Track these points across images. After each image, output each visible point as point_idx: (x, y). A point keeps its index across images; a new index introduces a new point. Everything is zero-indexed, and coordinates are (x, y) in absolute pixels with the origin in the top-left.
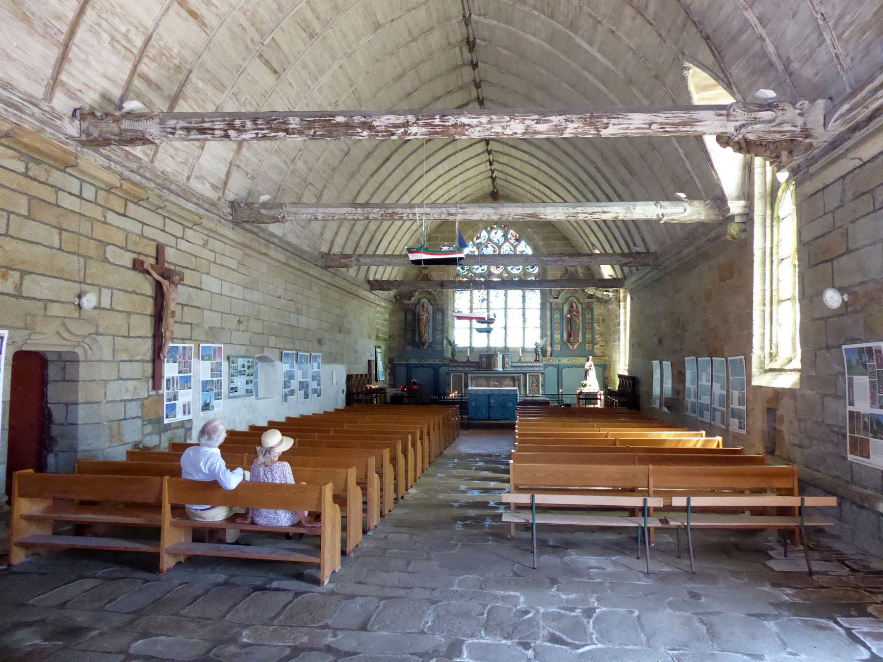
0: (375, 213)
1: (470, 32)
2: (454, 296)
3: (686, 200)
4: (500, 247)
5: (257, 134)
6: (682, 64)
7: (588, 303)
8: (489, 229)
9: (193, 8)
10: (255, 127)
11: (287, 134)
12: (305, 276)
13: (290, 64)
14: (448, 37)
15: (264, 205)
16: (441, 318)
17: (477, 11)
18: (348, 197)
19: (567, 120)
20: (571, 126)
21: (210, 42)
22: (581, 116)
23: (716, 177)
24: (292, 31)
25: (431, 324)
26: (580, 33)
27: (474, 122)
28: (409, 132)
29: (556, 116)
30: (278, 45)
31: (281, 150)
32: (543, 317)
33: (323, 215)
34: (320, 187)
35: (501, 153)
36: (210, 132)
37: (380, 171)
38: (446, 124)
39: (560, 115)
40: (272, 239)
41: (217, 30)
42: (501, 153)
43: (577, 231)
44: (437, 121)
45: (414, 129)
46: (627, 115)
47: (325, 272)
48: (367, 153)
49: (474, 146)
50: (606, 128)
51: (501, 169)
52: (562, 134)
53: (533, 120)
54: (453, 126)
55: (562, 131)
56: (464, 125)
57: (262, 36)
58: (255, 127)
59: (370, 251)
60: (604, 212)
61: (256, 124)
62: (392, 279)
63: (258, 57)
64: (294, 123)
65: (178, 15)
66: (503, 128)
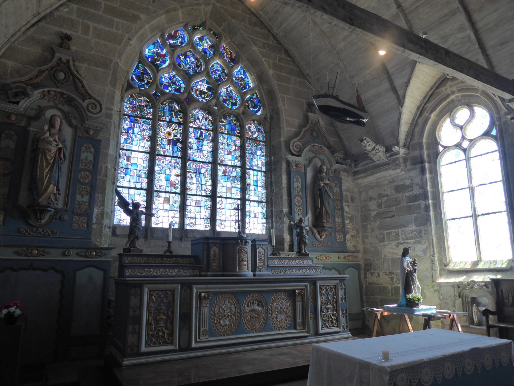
2: (120, 123)
4: (207, 63)
7: (335, 171)
8: (190, 28)
16: (91, 157)
25: (65, 167)
32: (269, 186)
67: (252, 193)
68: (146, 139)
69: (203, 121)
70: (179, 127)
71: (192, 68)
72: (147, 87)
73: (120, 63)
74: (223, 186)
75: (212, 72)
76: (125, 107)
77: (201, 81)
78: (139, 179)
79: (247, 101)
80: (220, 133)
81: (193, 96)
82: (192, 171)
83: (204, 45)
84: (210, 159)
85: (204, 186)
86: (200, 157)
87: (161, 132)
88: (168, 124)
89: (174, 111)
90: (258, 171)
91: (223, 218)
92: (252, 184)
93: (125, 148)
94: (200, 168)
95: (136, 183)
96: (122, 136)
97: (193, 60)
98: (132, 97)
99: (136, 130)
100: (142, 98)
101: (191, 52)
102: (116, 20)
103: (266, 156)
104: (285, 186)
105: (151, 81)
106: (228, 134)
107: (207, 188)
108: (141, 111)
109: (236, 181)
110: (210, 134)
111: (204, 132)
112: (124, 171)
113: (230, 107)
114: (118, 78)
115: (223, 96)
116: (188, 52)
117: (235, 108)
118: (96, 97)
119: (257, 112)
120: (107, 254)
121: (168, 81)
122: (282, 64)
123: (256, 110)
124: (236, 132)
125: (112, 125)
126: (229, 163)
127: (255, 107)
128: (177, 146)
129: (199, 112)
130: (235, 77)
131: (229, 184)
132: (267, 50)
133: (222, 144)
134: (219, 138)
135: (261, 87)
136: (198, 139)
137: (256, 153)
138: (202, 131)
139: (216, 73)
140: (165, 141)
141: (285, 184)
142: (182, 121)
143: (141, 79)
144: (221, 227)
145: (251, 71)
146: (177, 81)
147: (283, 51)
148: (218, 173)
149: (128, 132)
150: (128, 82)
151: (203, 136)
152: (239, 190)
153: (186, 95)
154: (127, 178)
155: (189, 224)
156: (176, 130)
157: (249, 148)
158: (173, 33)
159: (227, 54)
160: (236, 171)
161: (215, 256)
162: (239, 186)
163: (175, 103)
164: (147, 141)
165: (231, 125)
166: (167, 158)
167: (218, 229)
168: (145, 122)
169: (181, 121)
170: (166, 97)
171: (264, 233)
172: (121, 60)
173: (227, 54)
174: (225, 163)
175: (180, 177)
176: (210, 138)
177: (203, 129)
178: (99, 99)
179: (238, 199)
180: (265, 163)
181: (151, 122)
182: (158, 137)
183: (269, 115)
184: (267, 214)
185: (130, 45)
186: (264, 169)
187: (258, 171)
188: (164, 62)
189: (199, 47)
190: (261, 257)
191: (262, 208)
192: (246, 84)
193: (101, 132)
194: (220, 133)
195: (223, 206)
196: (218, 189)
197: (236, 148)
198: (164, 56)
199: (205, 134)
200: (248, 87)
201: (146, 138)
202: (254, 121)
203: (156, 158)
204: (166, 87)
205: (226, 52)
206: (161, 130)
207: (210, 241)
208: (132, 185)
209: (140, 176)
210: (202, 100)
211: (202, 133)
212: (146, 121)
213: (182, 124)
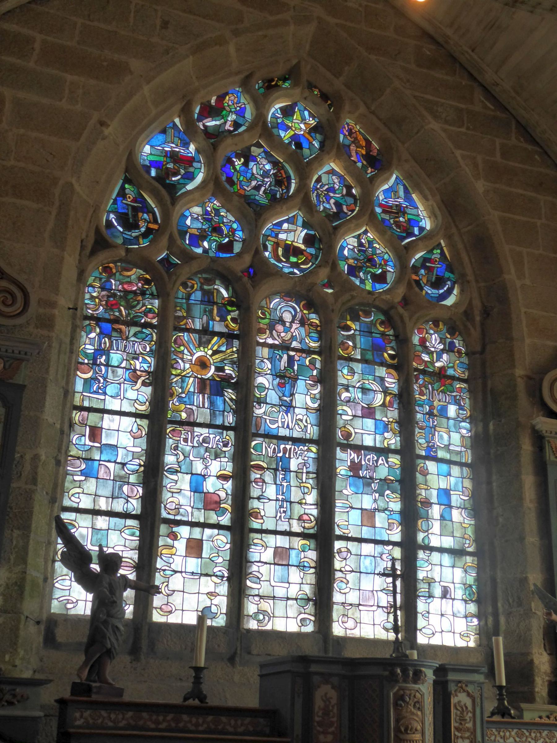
2: (74, 339)
8: (258, 85)
67: (436, 527)
68: (143, 378)
69: (294, 326)
70: (229, 345)
71: (263, 189)
72: (144, 243)
73: (77, 187)
74: (352, 508)
75: (318, 196)
76: (87, 296)
77: (287, 221)
78: (121, 488)
79: (415, 269)
80: (341, 358)
81: (265, 261)
82: (265, 465)
83: (297, 125)
84: (313, 432)
85: (297, 507)
86: (288, 426)
87: (182, 359)
88: (200, 338)
89: (217, 303)
90: (449, 462)
91: (353, 597)
92: (434, 500)
93: (86, 404)
94: (287, 456)
95: (113, 498)
96: (78, 373)
97: (268, 167)
98: (107, 269)
99: (116, 358)
100: (134, 273)
101: (258, 145)
102: (69, 77)
103: (472, 419)
104: (531, 506)
105: (155, 227)
106: (364, 361)
107: (307, 511)
108: (129, 307)
109: (388, 492)
110: (313, 362)
111: (297, 358)
112: (83, 466)
113: (369, 287)
114: (70, 223)
115: (347, 258)
116: (253, 148)
117: (380, 288)
118: (15, 275)
120: (28, 698)
121: (199, 225)
122: (511, 163)
123: (441, 291)
124: (386, 355)
125: (54, 345)
126: (368, 441)
127: (438, 283)
128: (222, 395)
129: (283, 304)
130: (381, 205)
131: (367, 502)
132: (468, 128)
133: (347, 390)
134: (340, 373)
135: (454, 230)
136: (282, 377)
137: (443, 413)
138: (292, 353)
139: (328, 198)
140: (191, 384)
141: (531, 501)
142: (237, 328)
144: (346, 625)
145: (425, 187)
146: (223, 223)
147: (514, 127)
148: (338, 471)
149: (95, 363)
150: (98, 231)
151: (296, 368)
152: (397, 517)
153: (247, 259)
154: (91, 485)
155: (256, 614)
156: (221, 355)
157: (425, 397)
158: (213, 102)
159: (357, 147)
160: (387, 462)
161: (326, 712)
162: (396, 506)
163: (217, 282)
164: (144, 384)
165: (372, 337)
166: (196, 429)
167: (337, 630)
168: (140, 335)
169: (234, 330)
170: (195, 266)
171: (472, 644)
172: (79, 177)
173: (357, 147)
174: (355, 440)
175: (230, 482)
176: (315, 373)
177: (294, 349)
178: (21, 279)
179: (394, 544)
180: (469, 439)
181: (154, 335)
182: (174, 372)
183: (477, 303)
184: (478, 587)
185: (103, 139)
186: (468, 458)
187: (449, 462)
188: (190, 177)
189: (282, 134)
190: (462, 720)
191: (466, 571)
192: (412, 222)
193: (24, 363)
194: (341, 358)
195: (351, 563)
196: (337, 514)
197: (388, 398)
198: (190, 161)
199: (299, 363)
200: (416, 231)
201: (140, 376)
202: (436, 323)
203: (168, 431)
204: (196, 240)
205: (356, 141)
206: (180, 356)
207: (314, 668)
208: (103, 505)
209: (122, 480)
210: (291, 270)
211: (291, 360)
212: (141, 332)
213: (236, 337)
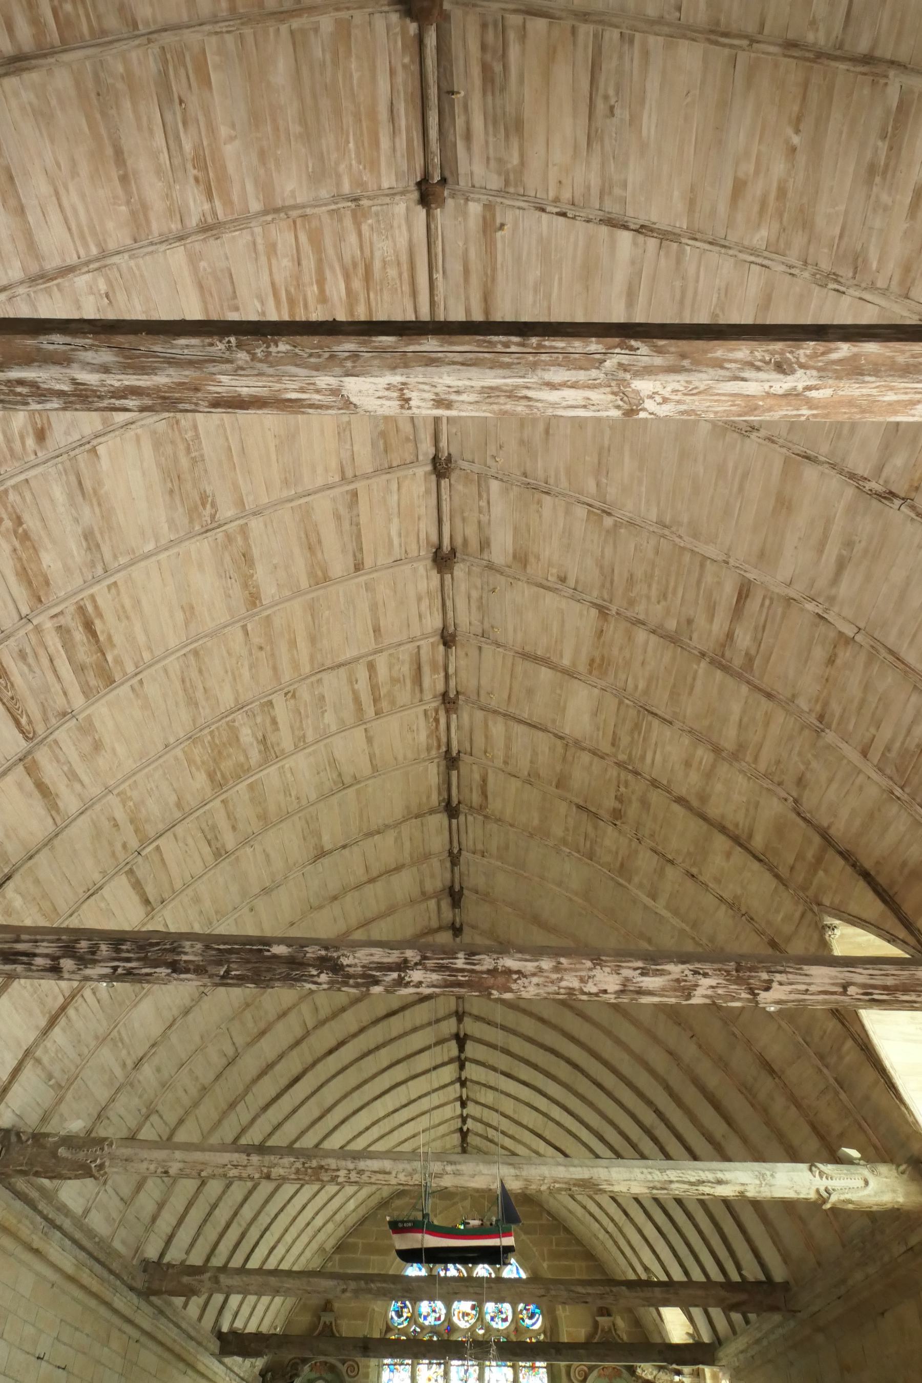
0: (284, 1166)
1: (457, 876)
2: (379, 1376)
3: (862, 1162)
5: (115, 968)
6: (821, 920)
9: (47, 781)
10: (114, 955)
11: (174, 971)
12: (103, 1311)
13: (174, 892)
14: (422, 882)
15: (68, 1141)
17: (471, 843)
18: (227, 1132)
19: (696, 972)
20: (705, 982)
21: (57, 835)
22: (720, 966)
23: (910, 1119)
24: (190, 841)
26: (636, 880)
27: (530, 966)
28: (407, 979)
29: (676, 963)
30: (163, 860)
31: (122, 1040)
33: (181, 1165)
34: (172, 1119)
35: (484, 1085)
36: (25, 959)
37: (280, 1101)
38: (477, 968)
39: (683, 963)
40: (60, 1220)
41: (75, 819)
42: (484, 1085)
43: (616, 1243)
44: (460, 963)
45: (416, 975)
46: (801, 969)
47: (144, 1305)
48: (264, 1065)
49: (440, 1070)
50: (767, 989)
51: (478, 1115)
52: (689, 997)
53: (635, 969)
54: (489, 972)
55: (688, 992)
56: (508, 972)
57: (141, 842)
58: (114, 955)
59: (236, 1262)
60: (720, 1182)
61: (118, 951)
62: (264, 1329)
63: (126, 873)
64: (191, 954)
65: (20, 786)
66: (582, 980)
73: (376, 1309)
79: (521, 1312)
119: (533, 1324)
127: (531, 1318)
143: (400, 1315)
150: (387, 1324)
153: (446, 1324)
170: (425, 1332)
183: (548, 1326)
204: (425, 1318)
